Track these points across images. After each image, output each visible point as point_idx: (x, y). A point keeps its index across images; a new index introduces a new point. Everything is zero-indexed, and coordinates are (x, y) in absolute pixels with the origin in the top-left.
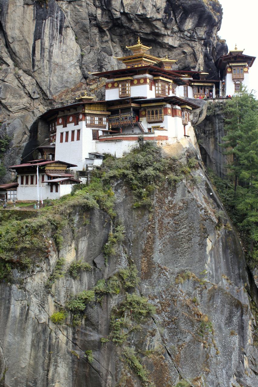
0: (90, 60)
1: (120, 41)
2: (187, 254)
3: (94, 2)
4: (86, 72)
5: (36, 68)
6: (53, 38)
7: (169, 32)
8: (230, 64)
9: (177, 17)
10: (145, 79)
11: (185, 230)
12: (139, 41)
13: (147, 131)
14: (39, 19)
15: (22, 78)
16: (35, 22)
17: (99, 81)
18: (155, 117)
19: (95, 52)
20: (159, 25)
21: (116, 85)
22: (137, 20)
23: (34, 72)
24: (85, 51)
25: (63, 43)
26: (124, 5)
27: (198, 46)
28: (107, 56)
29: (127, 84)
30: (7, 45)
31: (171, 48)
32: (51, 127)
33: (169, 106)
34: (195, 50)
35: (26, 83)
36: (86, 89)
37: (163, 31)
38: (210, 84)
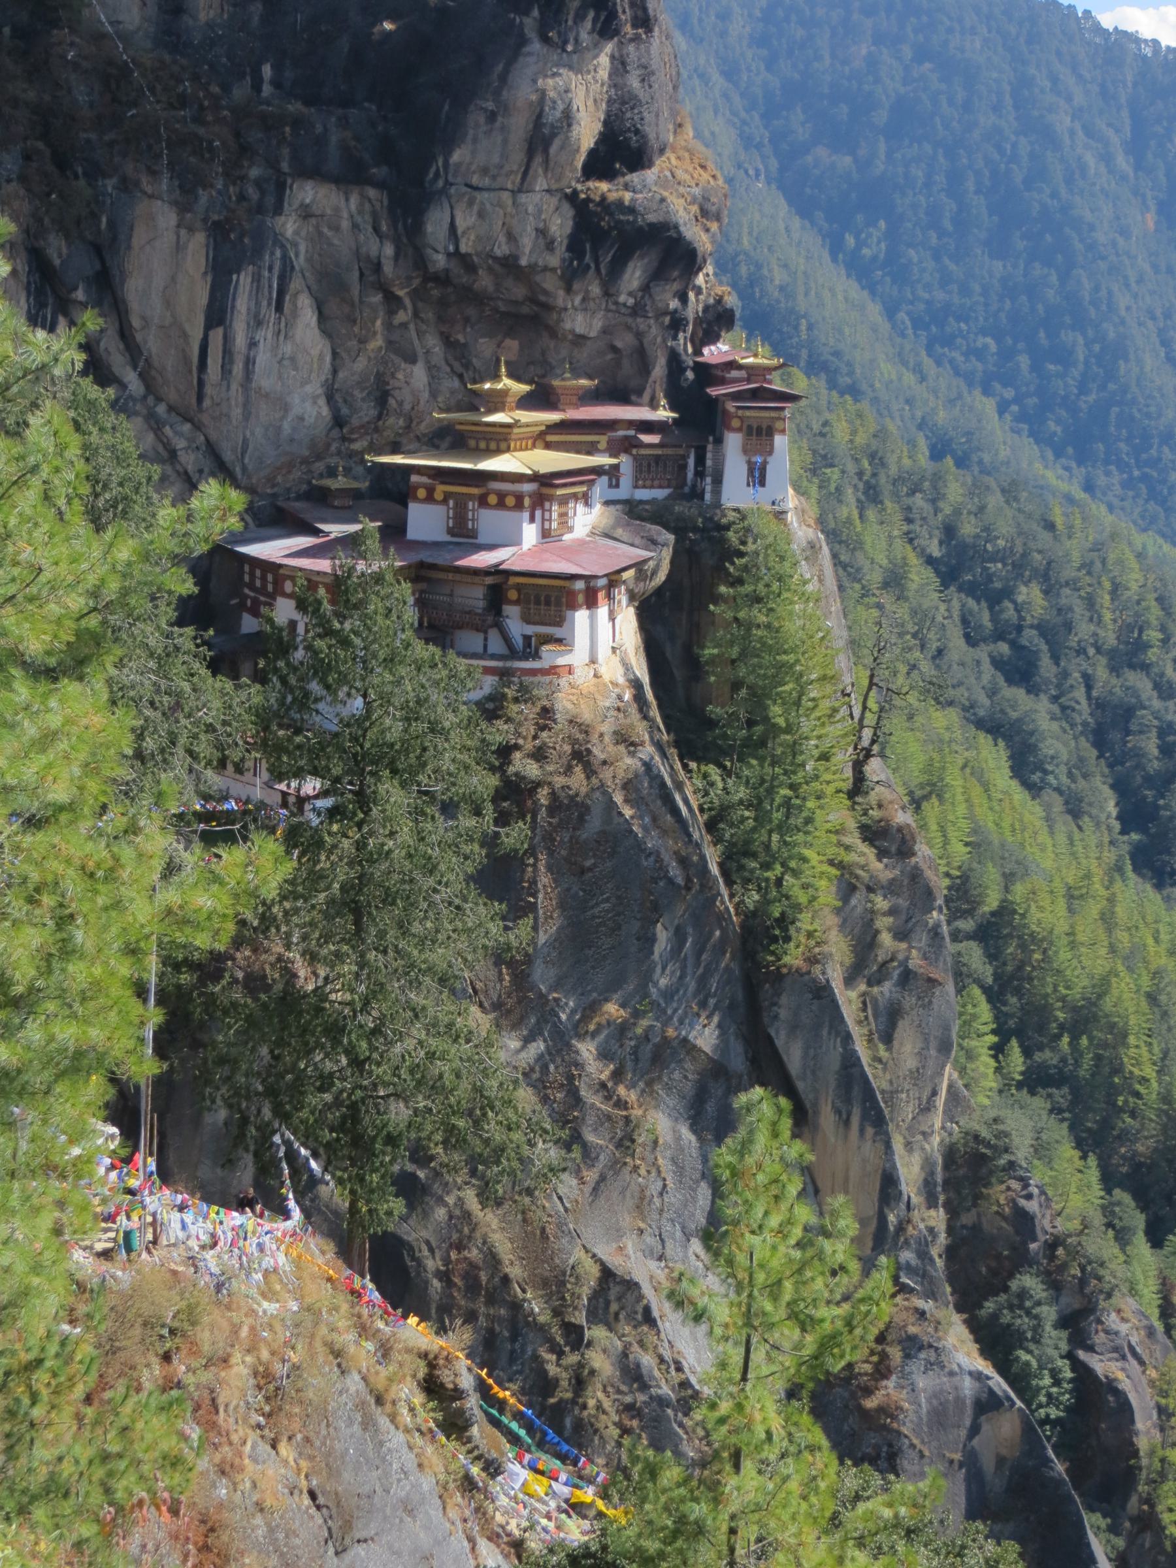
1: (441, 319)
4: (345, 411)
5: (207, 403)
6: (259, 323)
7: (578, 300)
10: (519, 498)
11: (606, 906)
13: (519, 642)
14: (221, 274)
15: (167, 430)
16: (209, 279)
17: (376, 430)
20: (550, 283)
21: (439, 495)
22: (490, 269)
23: (200, 408)
27: (654, 331)
30: (125, 334)
31: (580, 340)
32: (247, 568)
33: (580, 585)
34: (646, 341)
35: (180, 444)
36: (339, 453)
37: (560, 298)
38: (681, 452)
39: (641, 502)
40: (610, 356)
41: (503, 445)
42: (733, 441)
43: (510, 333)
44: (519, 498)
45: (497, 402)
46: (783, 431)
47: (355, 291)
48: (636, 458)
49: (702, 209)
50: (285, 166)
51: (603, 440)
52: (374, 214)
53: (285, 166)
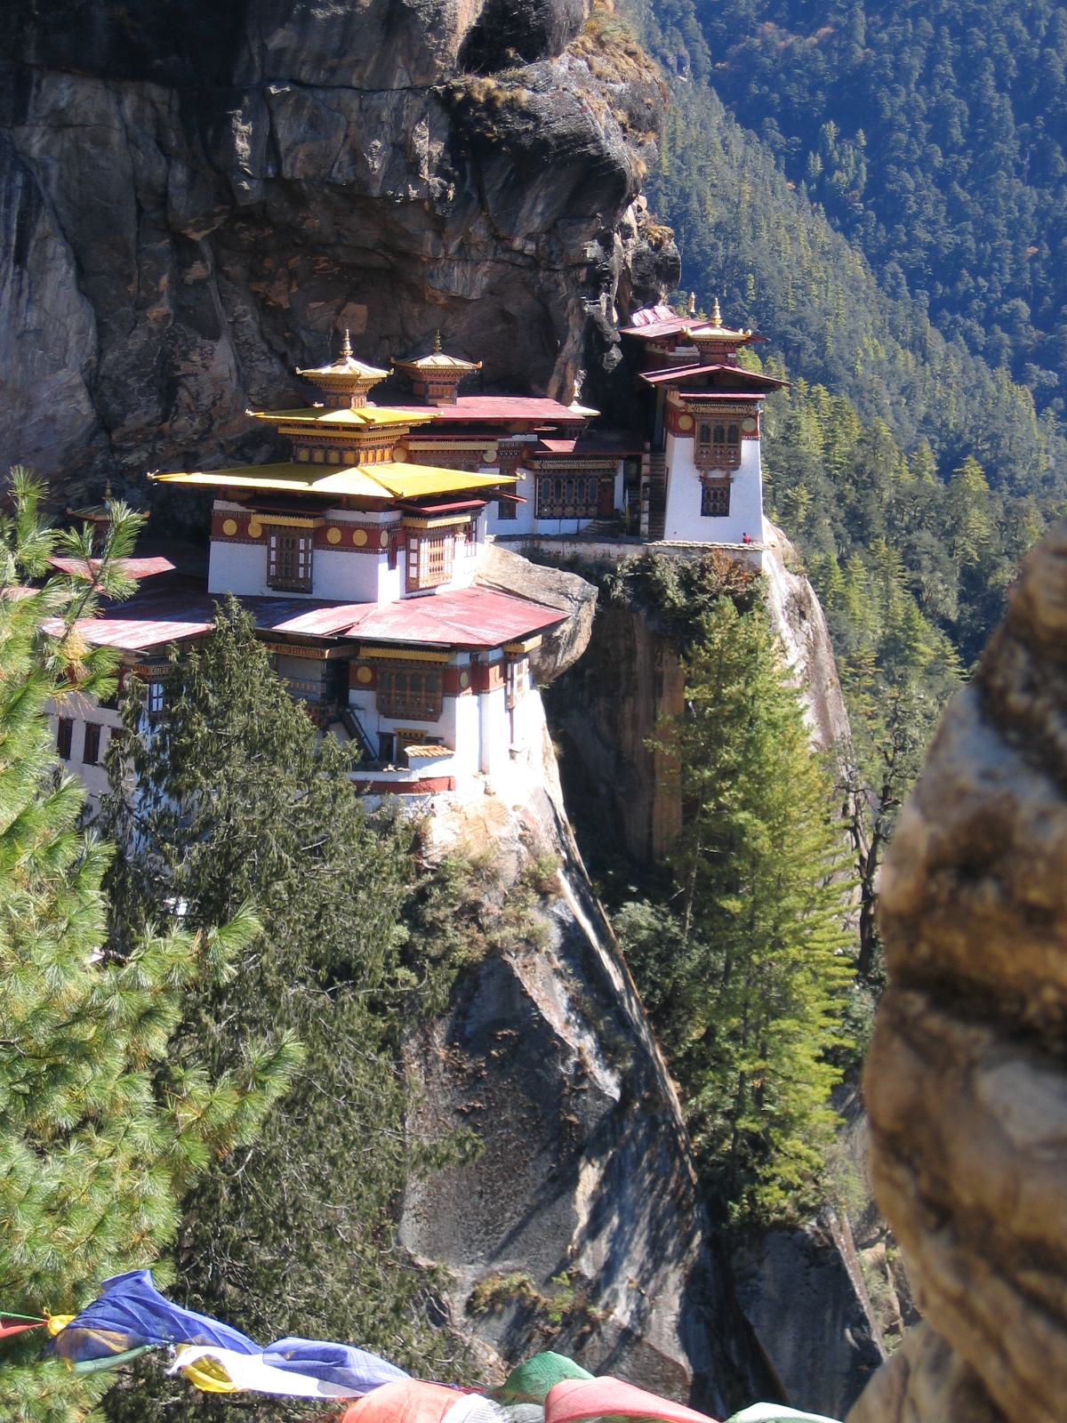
0: (130, 359)
1: (254, 274)
2: (508, 1215)
3: (158, 135)
4: (115, 407)
8: (691, 408)
9: (487, 187)
12: (348, 347)
17: (160, 435)
18: (408, 700)
19: (151, 332)
21: (254, 530)
24: (114, 327)
25: (29, 301)
26: (282, 149)
27: (564, 289)
28: (199, 339)
29: (302, 541)
31: (458, 303)
33: (463, 659)
34: (550, 305)
39: (548, 538)
40: (499, 328)
41: (349, 457)
42: (681, 450)
43: (354, 295)
44: (373, 531)
45: (338, 393)
46: (752, 435)
47: (133, 236)
48: (539, 476)
49: (631, 116)
50: (31, 56)
51: (491, 448)
52: (159, 124)
53: (31, 56)
